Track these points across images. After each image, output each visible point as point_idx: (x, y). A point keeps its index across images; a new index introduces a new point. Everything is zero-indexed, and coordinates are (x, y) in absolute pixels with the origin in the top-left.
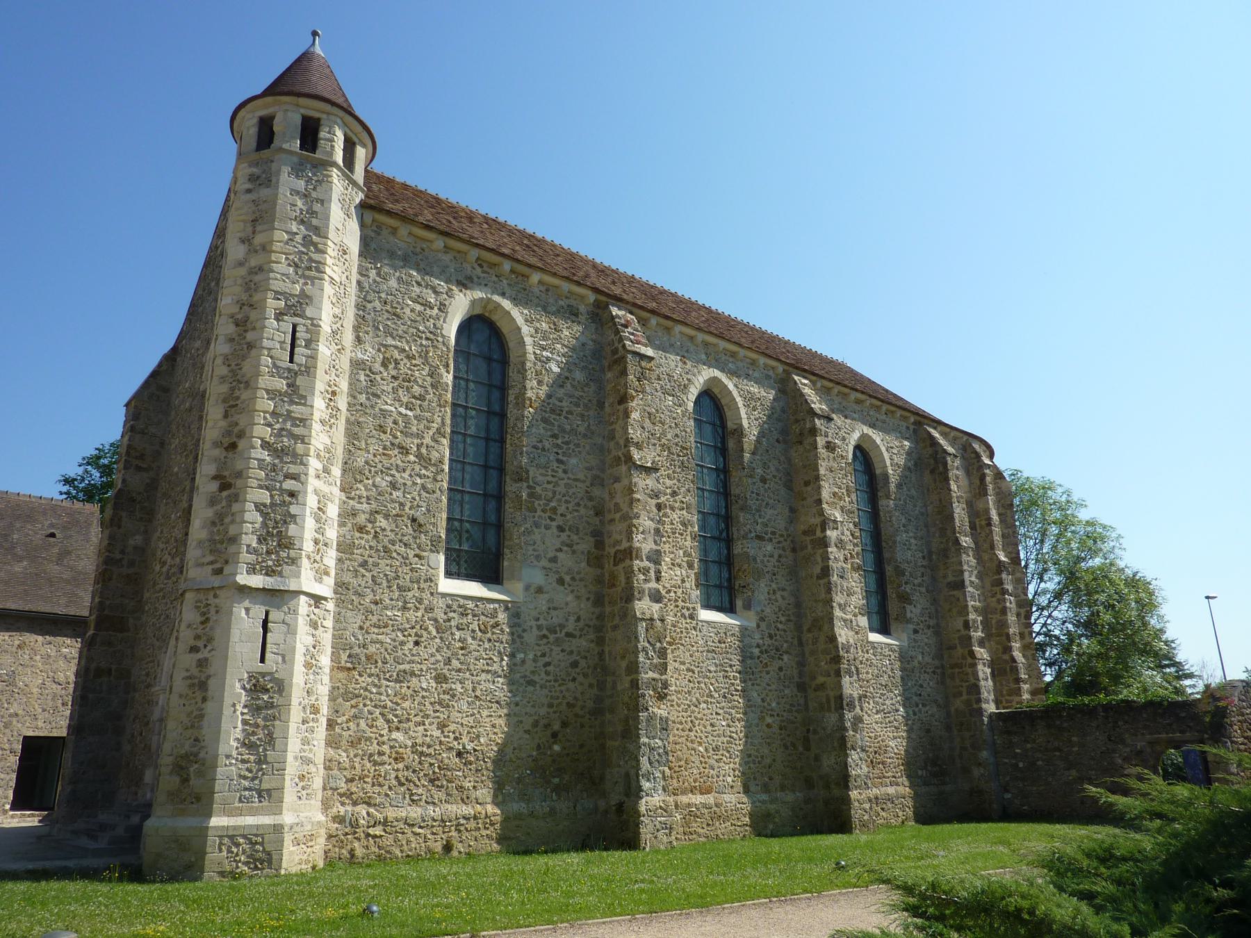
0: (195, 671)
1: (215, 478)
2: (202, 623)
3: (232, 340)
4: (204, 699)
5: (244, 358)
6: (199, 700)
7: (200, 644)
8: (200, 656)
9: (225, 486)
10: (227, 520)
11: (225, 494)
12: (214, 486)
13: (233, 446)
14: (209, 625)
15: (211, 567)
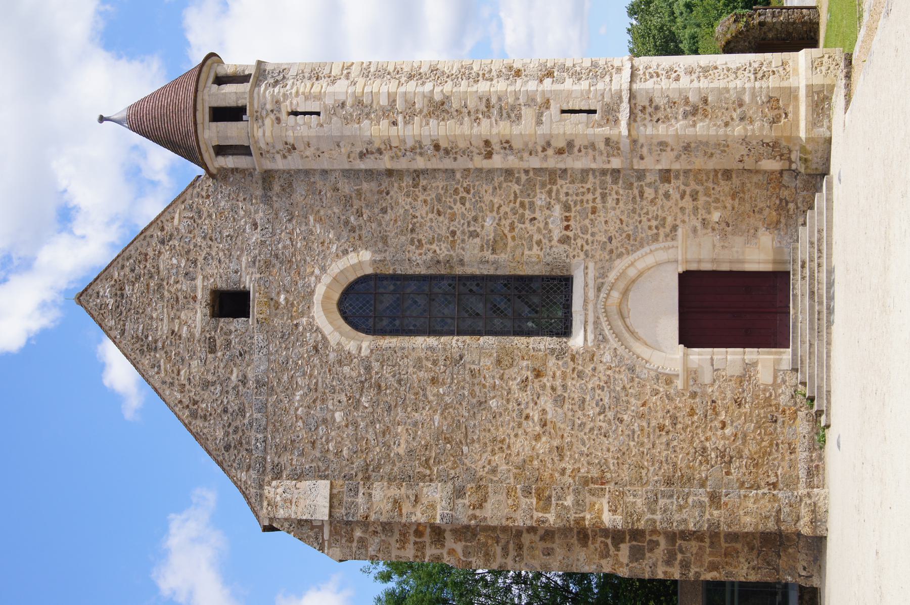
0: (694, 76)
1: (541, 81)
2: (658, 76)
3: (423, 84)
4: (716, 68)
5: (443, 73)
6: (715, 71)
7: (674, 75)
8: (682, 75)
9: (550, 74)
10: (578, 69)
11: (555, 75)
12: (548, 81)
13: (518, 73)
14: (660, 72)
15: (614, 76)
